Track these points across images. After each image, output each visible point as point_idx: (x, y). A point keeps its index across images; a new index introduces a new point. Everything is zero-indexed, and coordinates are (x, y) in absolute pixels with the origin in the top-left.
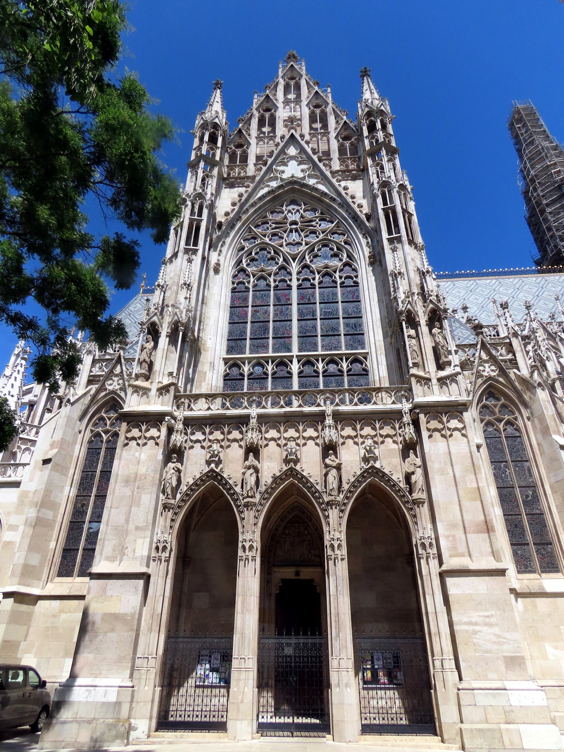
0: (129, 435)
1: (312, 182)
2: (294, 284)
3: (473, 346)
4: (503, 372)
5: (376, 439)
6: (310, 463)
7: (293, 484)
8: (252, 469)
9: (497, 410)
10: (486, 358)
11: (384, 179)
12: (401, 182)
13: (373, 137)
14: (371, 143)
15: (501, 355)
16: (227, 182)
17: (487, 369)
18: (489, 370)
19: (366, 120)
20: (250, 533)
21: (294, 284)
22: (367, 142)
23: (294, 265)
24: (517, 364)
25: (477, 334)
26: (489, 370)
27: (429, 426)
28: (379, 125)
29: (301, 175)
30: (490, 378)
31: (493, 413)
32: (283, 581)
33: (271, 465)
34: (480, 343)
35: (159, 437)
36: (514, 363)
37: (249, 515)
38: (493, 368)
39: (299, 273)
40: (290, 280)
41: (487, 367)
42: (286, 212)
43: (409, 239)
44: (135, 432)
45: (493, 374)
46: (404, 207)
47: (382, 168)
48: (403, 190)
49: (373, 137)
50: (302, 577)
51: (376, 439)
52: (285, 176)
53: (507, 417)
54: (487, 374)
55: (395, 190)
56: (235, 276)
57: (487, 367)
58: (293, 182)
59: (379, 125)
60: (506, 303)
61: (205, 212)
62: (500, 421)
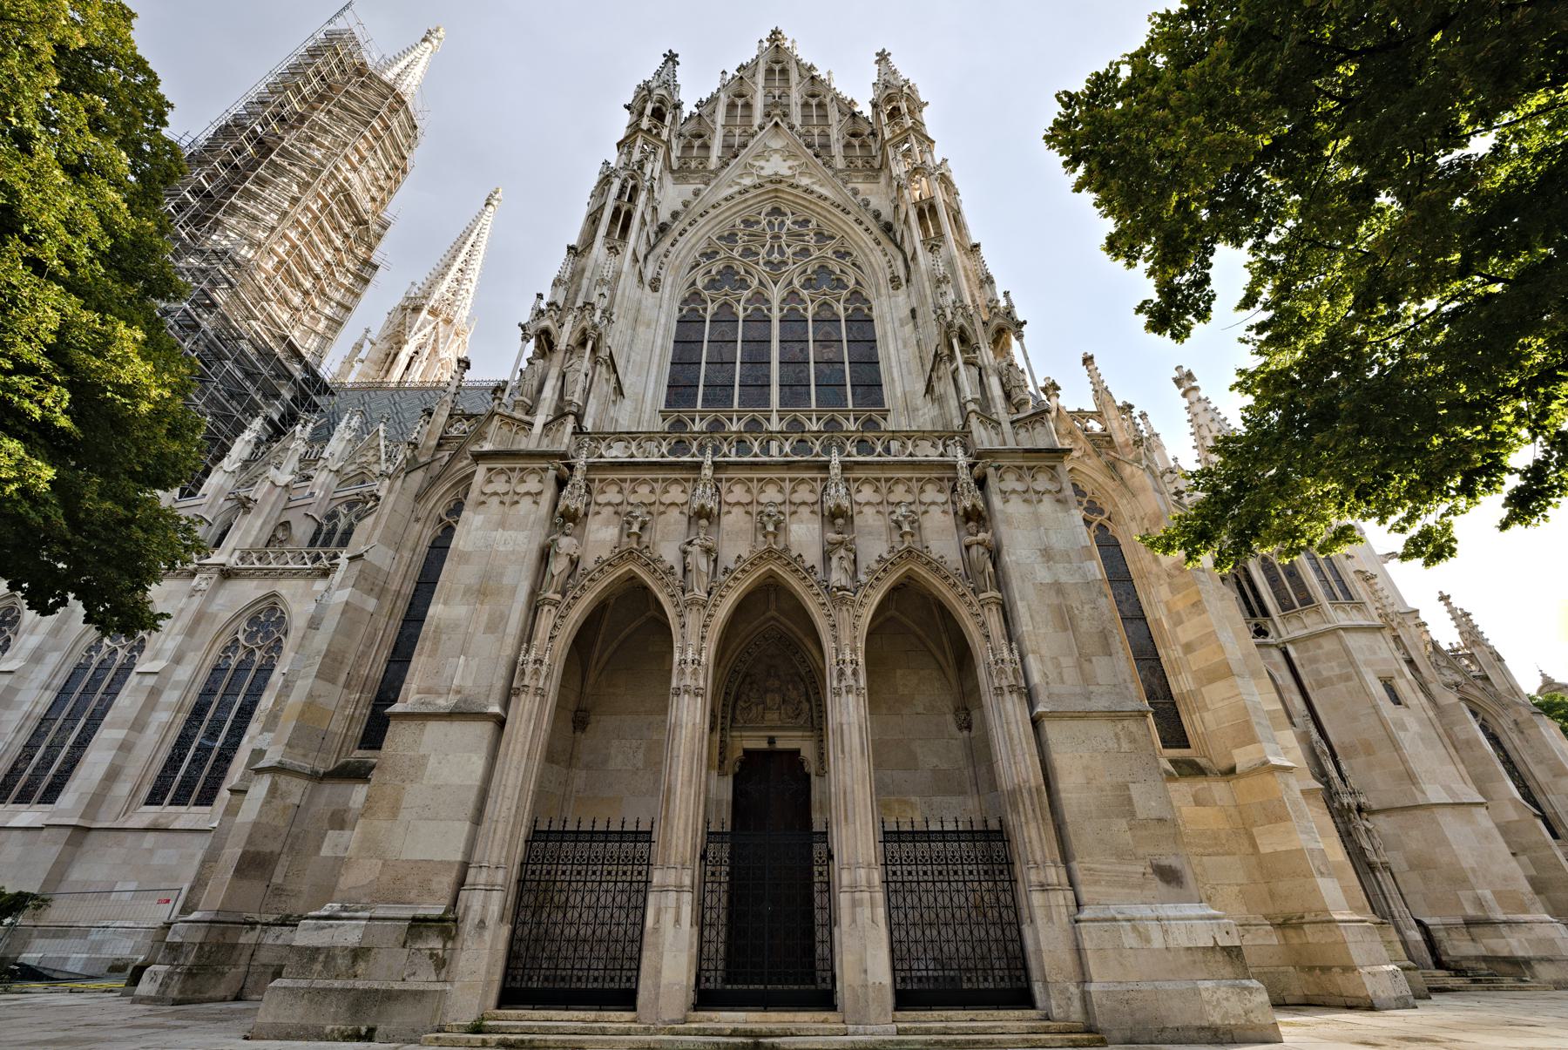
0: (489, 489)
1: (805, 181)
2: (776, 315)
5: (913, 508)
6: (805, 535)
7: (771, 575)
8: (700, 552)
16: (681, 173)
20: (695, 646)
21: (776, 315)
23: (775, 290)
27: (1004, 486)
29: (789, 173)
32: (747, 752)
33: (736, 539)
35: (540, 493)
37: (693, 619)
39: (784, 300)
40: (769, 310)
42: (764, 222)
44: (500, 485)
50: (781, 745)
51: (913, 508)
52: (763, 173)
56: (685, 302)
58: (777, 180)
60: (1092, 358)
61: (642, 197)
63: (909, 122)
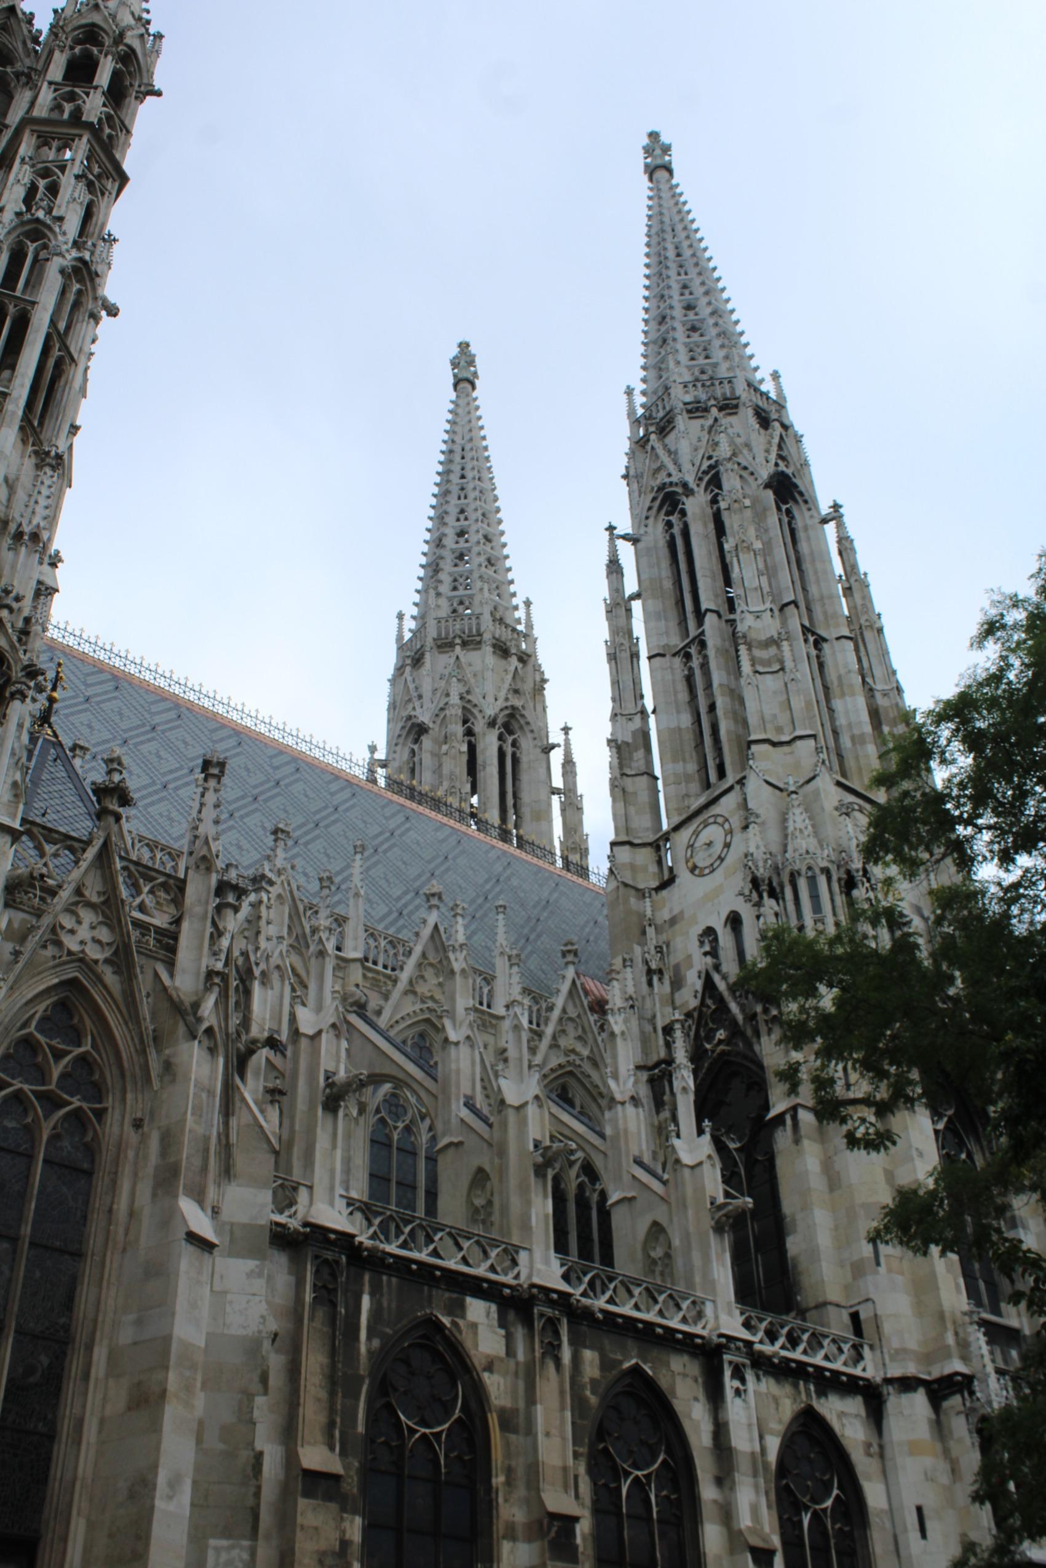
3: (74, 845)
4: (122, 959)
9: (56, 1071)
10: (95, 899)
11: (41, 214)
12: (87, 256)
13: (72, 97)
14: (57, 107)
15: (142, 908)
17: (84, 933)
18: (85, 935)
19: (77, 41)
22: (46, 96)
24: (173, 950)
25: (101, 814)
26: (85, 935)
28: (103, 77)
30: (81, 960)
31: (42, 1076)
34: (97, 844)
36: (168, 943)
38: (104, 934)
41: (86, 925)
43: (26, 418)
45: (94, 953)
46: (62, 326)
47: (53, 190)
48: (80, 281)
49: (72, 97)
53: (76, 1102)
54: (75, 948)
55: (56, 263)
57: (86, 925)
59: (103, 77)
62: (51, 1102)
63: (94, 106)
